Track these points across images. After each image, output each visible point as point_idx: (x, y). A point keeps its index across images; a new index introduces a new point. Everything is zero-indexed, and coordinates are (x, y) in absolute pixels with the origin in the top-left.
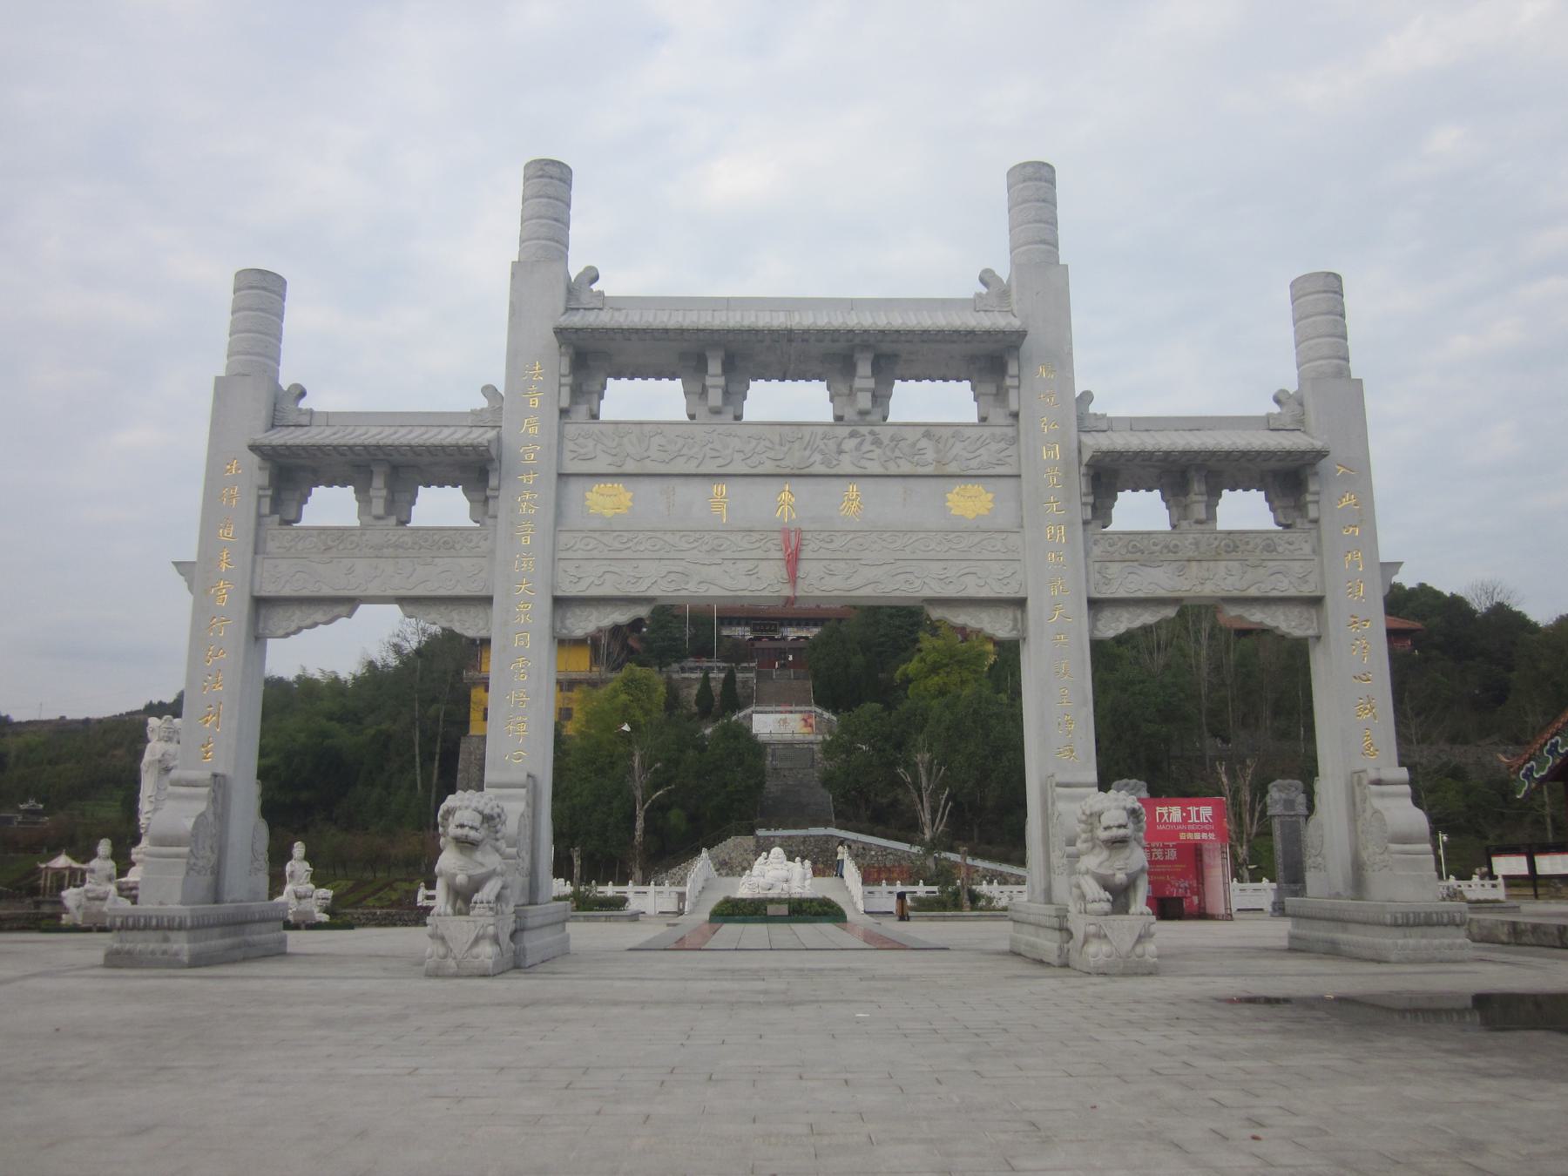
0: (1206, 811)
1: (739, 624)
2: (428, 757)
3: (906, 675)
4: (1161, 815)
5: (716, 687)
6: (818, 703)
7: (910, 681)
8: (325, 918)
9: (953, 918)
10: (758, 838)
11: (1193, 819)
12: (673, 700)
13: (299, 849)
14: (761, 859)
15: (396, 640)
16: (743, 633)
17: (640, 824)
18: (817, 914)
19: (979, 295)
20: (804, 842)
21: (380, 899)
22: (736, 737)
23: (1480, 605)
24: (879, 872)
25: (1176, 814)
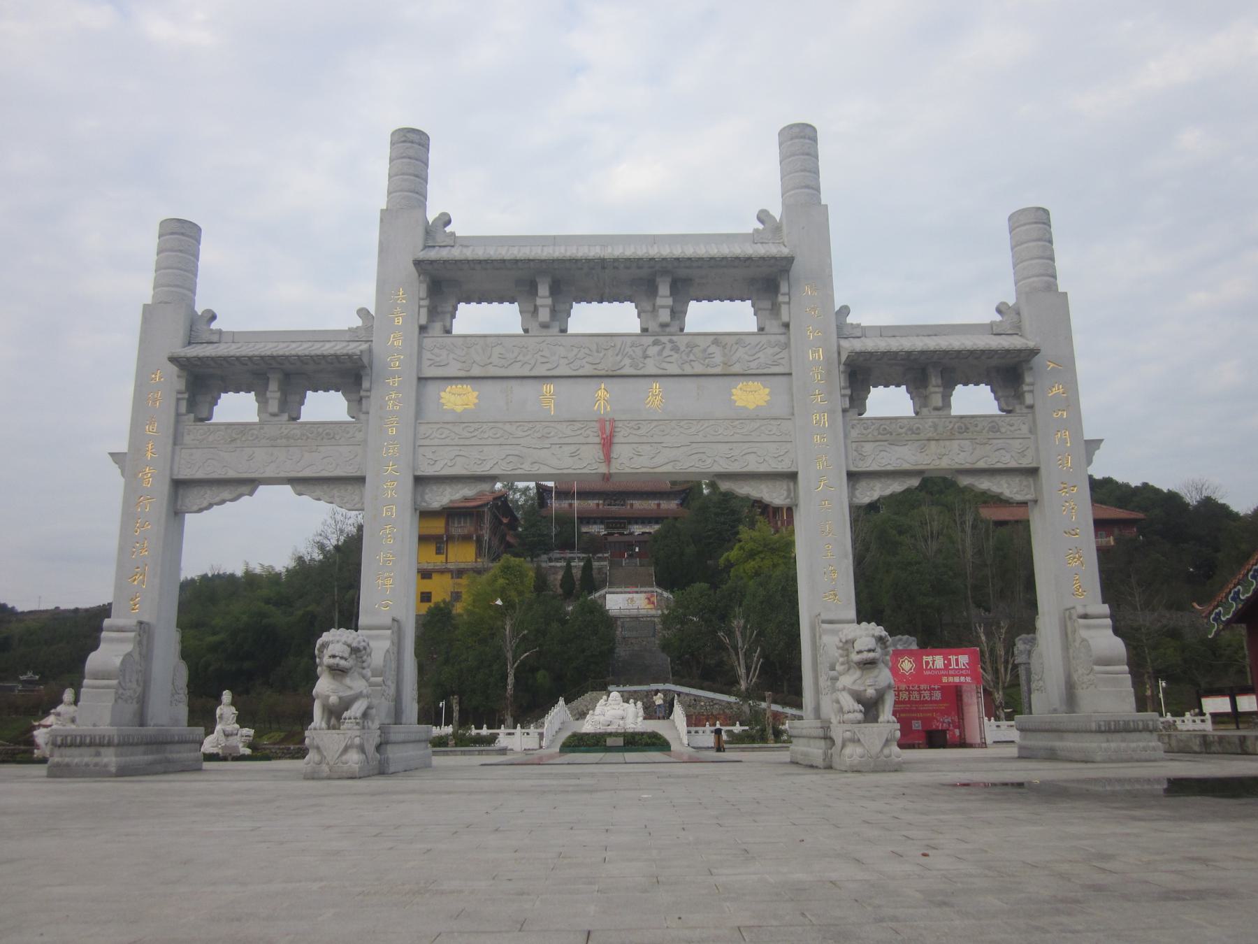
0: (964, 659)
1: (595, 523)
3: (728, 560)
4: (927, 663)
5: (577, 573)
6: (659, 585)
7: (732, 565)
8: (248, 751)
9: (760, 749)
11: (953, 665)
12: (541, 584)
13: (227, 696)
14: (602, 702)
15: (318, 539)
16: (598, 530)
17: (511, 680)
18: (647, 745)
19: (756, 230)
22: (591, 612)
23: (1192, 498)
25: (939, 661)
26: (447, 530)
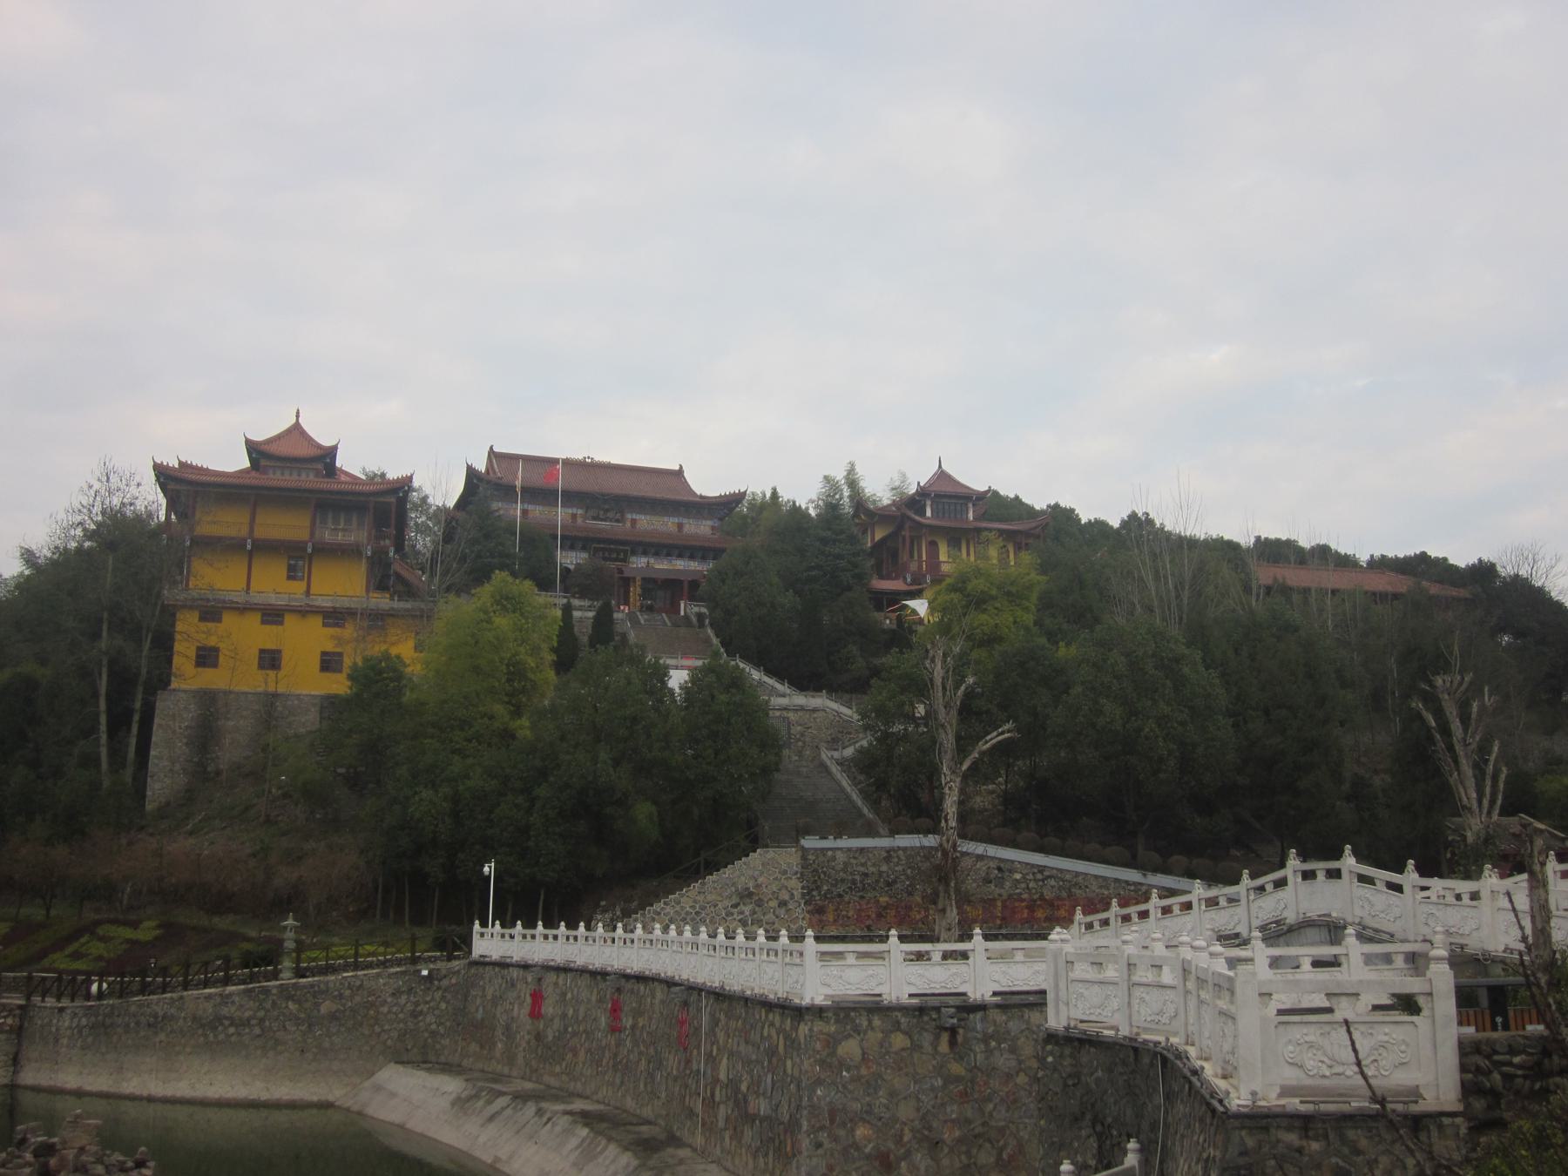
2: (118, 723)
5: (583, 632)
10: (804, 850)
16: (568, 559)
20: (888, 859)
21: (76, 956)
24: (1031, 908)
26: (312, 534)
